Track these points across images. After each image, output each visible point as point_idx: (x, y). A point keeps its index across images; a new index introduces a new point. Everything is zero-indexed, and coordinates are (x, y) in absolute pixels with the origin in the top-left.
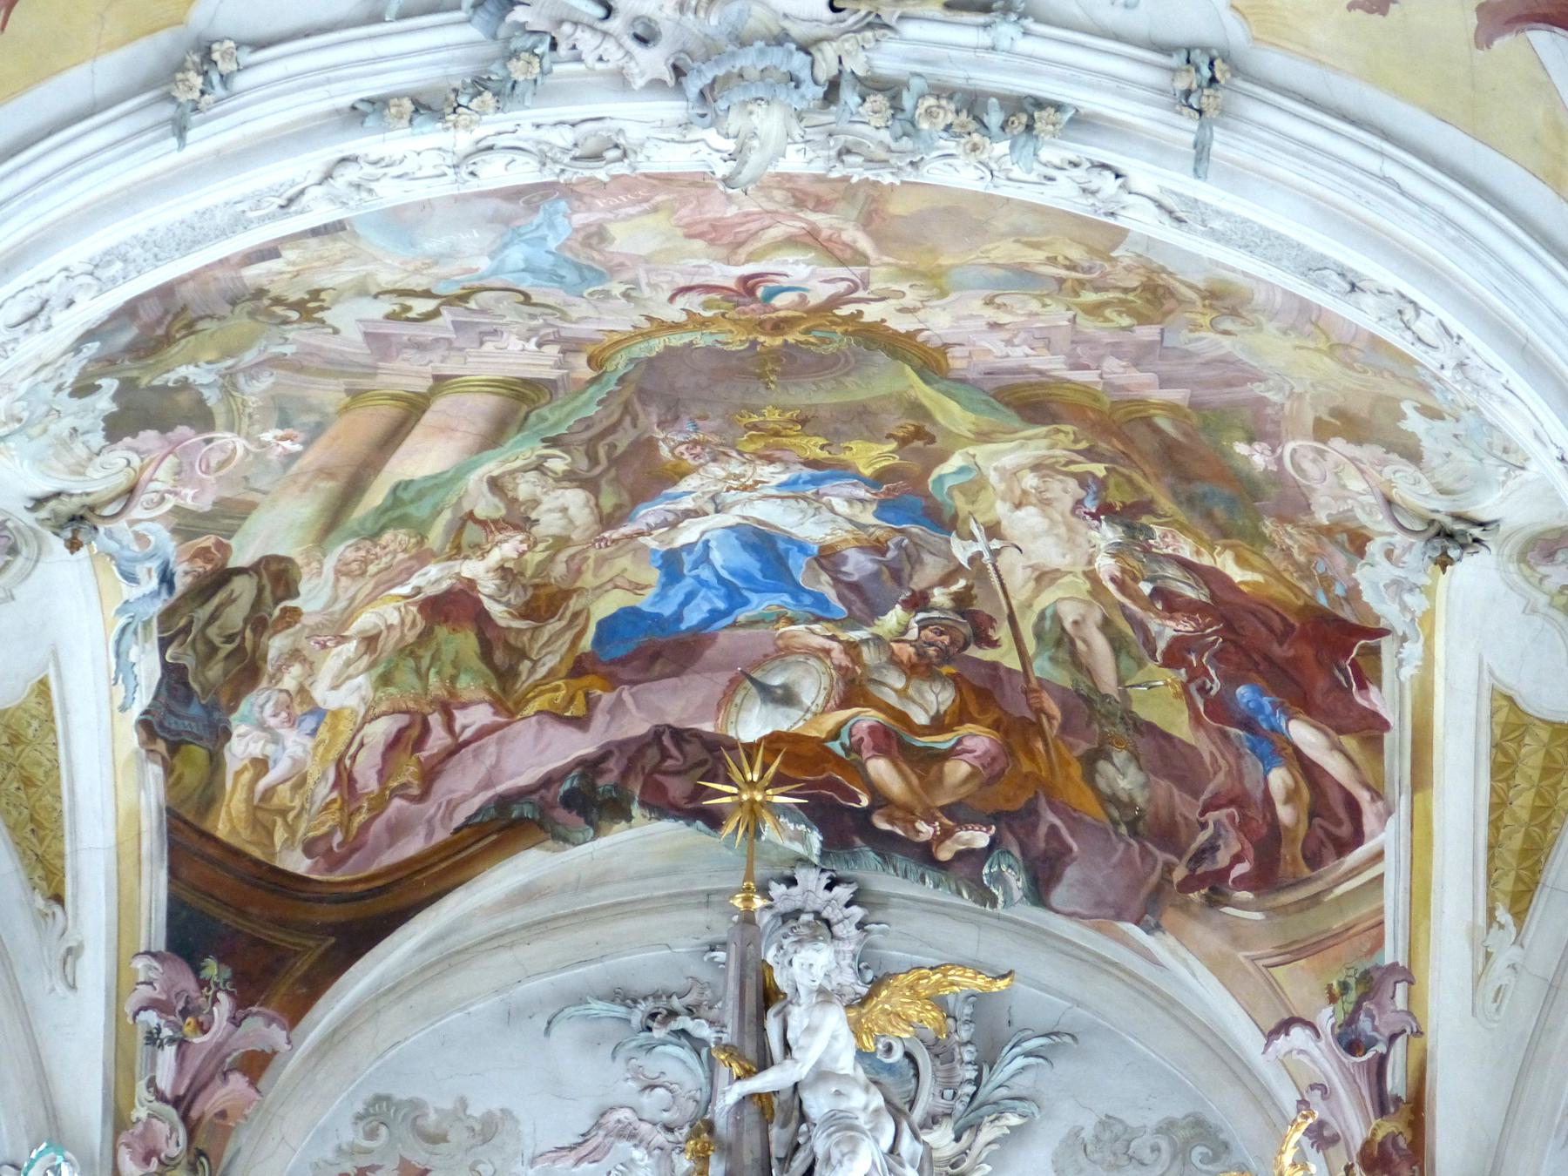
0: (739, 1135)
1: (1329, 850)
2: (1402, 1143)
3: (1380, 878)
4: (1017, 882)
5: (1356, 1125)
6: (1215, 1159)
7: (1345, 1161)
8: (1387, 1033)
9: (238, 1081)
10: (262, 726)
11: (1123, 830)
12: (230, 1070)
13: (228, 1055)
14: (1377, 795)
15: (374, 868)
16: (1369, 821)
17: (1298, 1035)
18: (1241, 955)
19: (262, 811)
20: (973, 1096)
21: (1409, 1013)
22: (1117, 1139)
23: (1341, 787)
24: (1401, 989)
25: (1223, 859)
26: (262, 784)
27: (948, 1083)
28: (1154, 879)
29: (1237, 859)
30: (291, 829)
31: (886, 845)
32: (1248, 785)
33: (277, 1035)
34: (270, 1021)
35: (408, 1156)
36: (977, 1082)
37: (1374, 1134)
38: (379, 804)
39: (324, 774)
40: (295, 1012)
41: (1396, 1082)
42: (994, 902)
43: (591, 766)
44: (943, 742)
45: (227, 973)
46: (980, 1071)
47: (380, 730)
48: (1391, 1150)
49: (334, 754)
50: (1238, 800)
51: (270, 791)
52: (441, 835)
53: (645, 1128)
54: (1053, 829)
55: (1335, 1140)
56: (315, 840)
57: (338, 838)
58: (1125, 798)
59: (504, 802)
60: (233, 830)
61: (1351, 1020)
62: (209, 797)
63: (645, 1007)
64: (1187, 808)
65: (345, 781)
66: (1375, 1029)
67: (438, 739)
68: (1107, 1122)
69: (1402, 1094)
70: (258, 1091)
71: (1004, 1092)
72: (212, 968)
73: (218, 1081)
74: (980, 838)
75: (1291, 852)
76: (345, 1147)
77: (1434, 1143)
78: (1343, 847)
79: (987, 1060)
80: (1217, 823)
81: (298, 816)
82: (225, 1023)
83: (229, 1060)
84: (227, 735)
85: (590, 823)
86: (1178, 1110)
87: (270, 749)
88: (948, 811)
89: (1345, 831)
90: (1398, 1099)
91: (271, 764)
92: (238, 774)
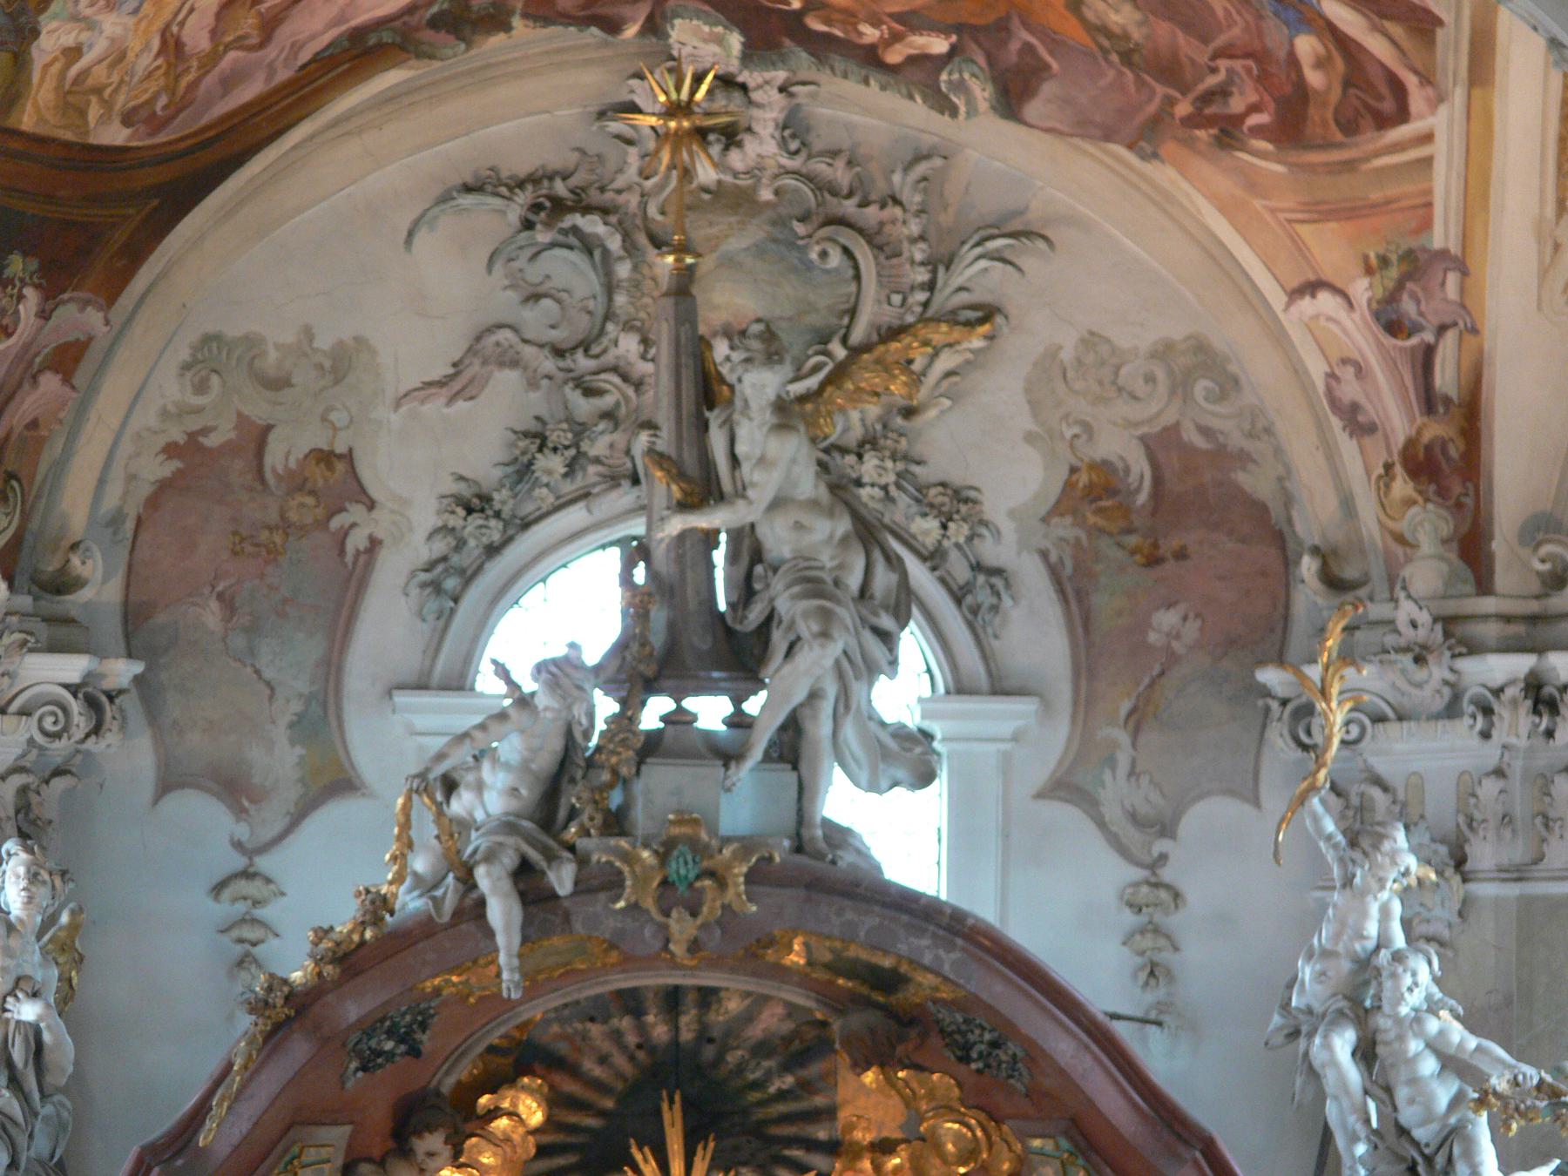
0: (682, 572)
1: (1367, 121)
2: (1453, 452)
3: (1427, 162)
4: (982, 92)
6: (1222, 397)
7: (1384, 457)
8: (1435, 320)
9: (50, 382)
10: (76, 18)
11: (1115, 58)
12: (40, 371)
13: (37, 354)
14: (1426, 80)
15: (205, 120)
16: (1417, 98)
17: (1325, 300)
18: (1258, 204)
19: (73, 98)
20: (926, 305)
21: (1463, 306)
22: (1103, 363)
23: (1383, 66)
24: (1452, 279)
25: (1237, 105)
26: (74, 70)
28: (1152, 108)
29: (1255, 108)
30: (108, 105)
31: (821, 47)
32: (1270, 43)
34: (85, 304)
35: (246, 411)
36: (931, 286)
37: (1419, 432)
39: (147, 47)
40: (111, 290)
41: (1445, 378)
42: (953, 111)
45: (34, 264)
46: (934, 272)
48: (1440, 457)
49: (159, 24)
50: (1260, 56)
51: (85, 73)
52: (283, 75)
53: (529, 351)
54: (1028, 49)
55: (1370, 429)
56: (135, 109)
57: (163, 101)
58: (1117, 30)
59: (358, 34)
60: (41, 120)
61: (1392, 298)
63: (524, 198)
64: (1190, 49)
65: (172, 47)
66: (1421, 314)
68: (1091, 340)
69: (1453, 393)
70: (73, 387)
71: (964, 297)
73: (26, 386)
74: (939, 45)
75: (1320, 118)
76: (170, 408)
77: (1491, 463)
78: (1384, 122)
79: (941, 262)
80: (1230, 71)
81: (116, 91)
82: (32, 319)
83: (38, 360)
84: (35, 33)
85: (461, 38)
86: (1177, 331)
87: (84, 37)
88: (899, 18)
89: (1388, 106)
90: (1447, 401)
91: (85, 49)
92: (47, 67)
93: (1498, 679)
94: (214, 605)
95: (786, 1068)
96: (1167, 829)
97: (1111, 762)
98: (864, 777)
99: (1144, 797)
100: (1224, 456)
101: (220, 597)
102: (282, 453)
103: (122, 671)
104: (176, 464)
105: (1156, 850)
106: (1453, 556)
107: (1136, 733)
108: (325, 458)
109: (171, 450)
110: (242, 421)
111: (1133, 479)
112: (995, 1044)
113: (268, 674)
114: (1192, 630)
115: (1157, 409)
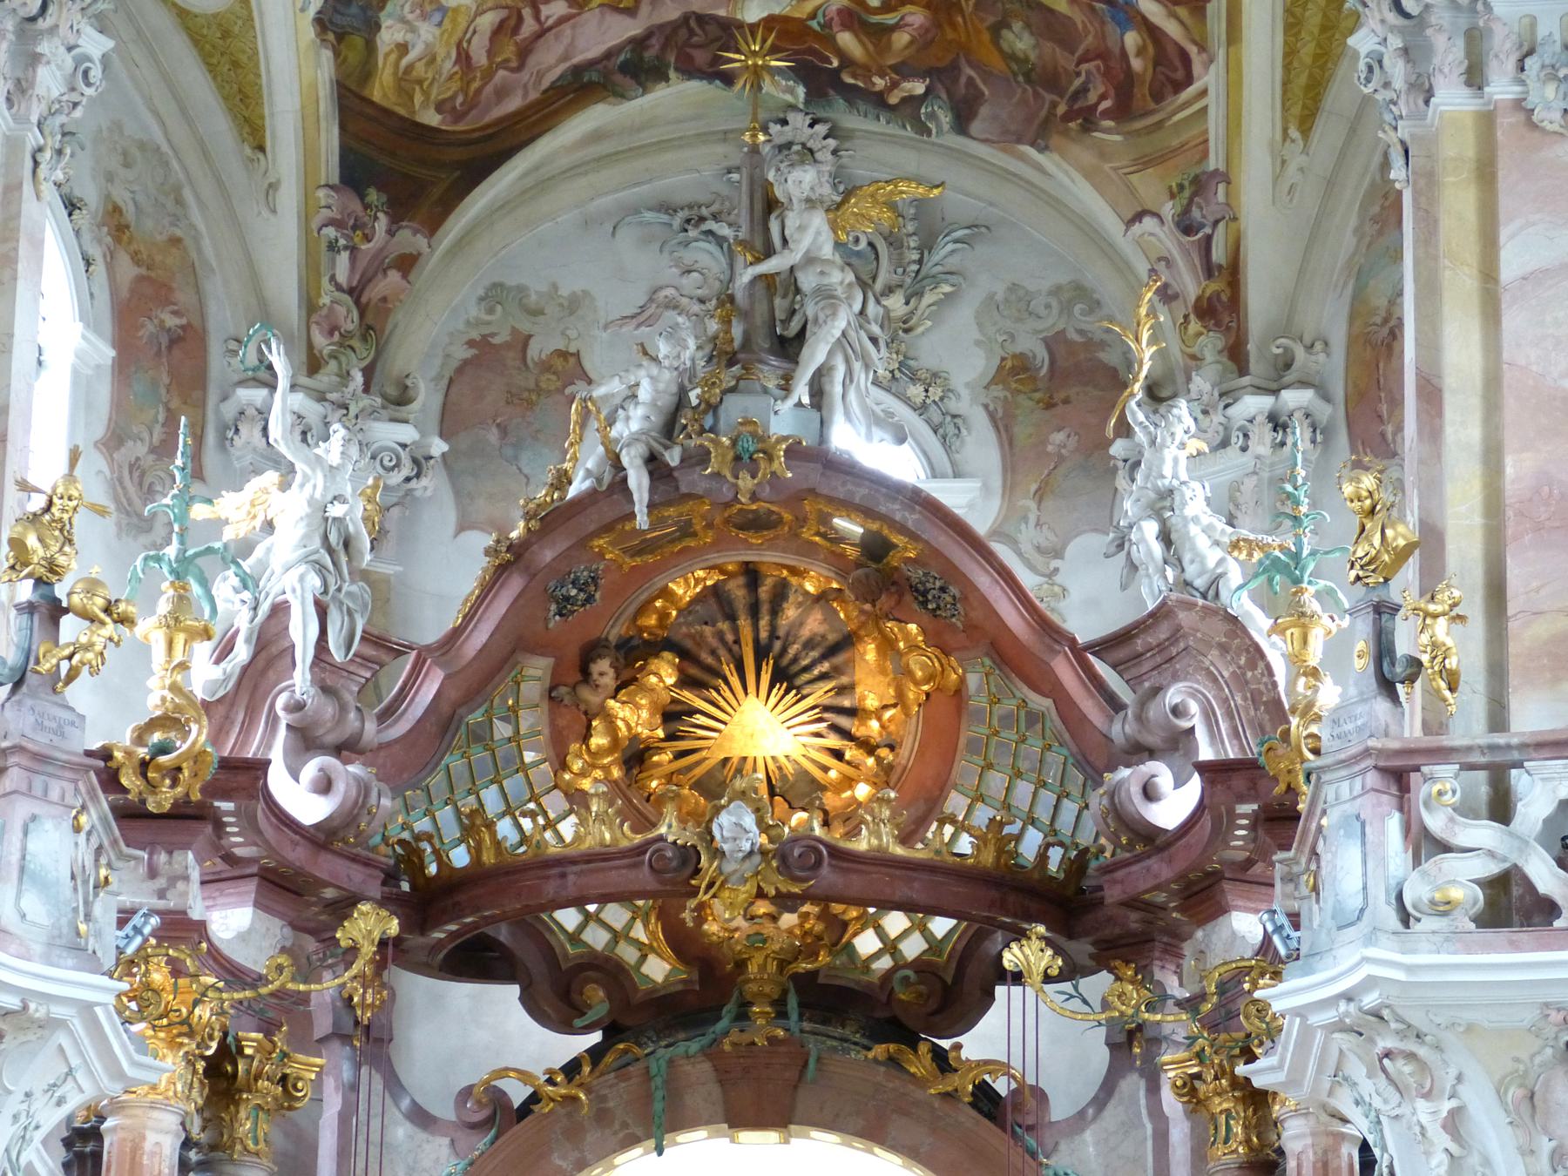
0: (752, 304)
1: (1169, 88)
2: (1224, 298)
3: (1205, 109)
4: (945, 118)
5: (1191, 286)
6: (1091, 311)
8: (1212, 219)
9: (394, 276)
10: (403, 20)
11: (1021, 78)
12: (389, 267)
14: (1202, 48)
15: (487, 119)
16: (1197, 68)
17: (1149, 223)
18: (1107, 166)
20: (918, 272)
21: (1228, 204)
22: (1020, 300)
23: (1176, 44)
24: (1221, 188)
25: (1092, 97)
26: (404, 62)
27: (899, 263)
28: (1043, 113)
29: (1103, 97)
30: (426, 94)
31: (852, 95)
32: (1110, 44)
33: (421, 242)
34: (415, 232)
36: (920, 262)
38: (489, 74)
39: (448, 54)
40: (433, 226)
41: (1219, 254)
42: (929, 133)
43: (639, 43)
44: (890, 19)
45: (384, 198)
46: (922, 254)
47: (488, 21)
49: (455, 39)
50: (1102, 55)
51: (410, 68)
52: (534, 95)
53: (685, 301)
54: (970, 80)
55: (1175, 297)
56: (444, 101)
57: (460, 99)
58: (1021, 55)
59: (578, 70)
60: (385, 95)
61: (1186, 211)
62: (367, 72)
63: (682, 215)
64: (1066, 61)
65: (464, 58)
66: (1204, 217)
67: (529, 27)
68: (1014, 288)
69: (1223, 262)
71: (939, 268)
72: (373, 196)
73: (380, 276)
74: (919, 88)
75: (1141, 92)
78: (1179, 87)
79: (927, 246)
80: (1088, 73)
81: (431, 84)
84: (378, 27)
85: (640, 84)
86: (1063, 278)
87: (409, 37)
88: (895, 68)
89: (1179, 75)
90: (1220, 267)
92: (387, 55)
93: (1252, 411)
94: (495, 430)
95: (824, 657)
96: (1058, 553)
97: (1025, 519)
98: (863, 430)
99: (1046, 537)
100: (1092, 345)
101: (498, 425)
102: (538, 349)
103: (438, 447)
104: (473, 352)
105: (1052, 567)
106: (1225, 360)
107: (1040, 502)
108: (563, 354)
109: (471, 343)
110: (514, 331)
111: (1038, 362)
112: (943, 589)
113: (526, 471)
114: (1072, 443)
115: (1052, 321)
